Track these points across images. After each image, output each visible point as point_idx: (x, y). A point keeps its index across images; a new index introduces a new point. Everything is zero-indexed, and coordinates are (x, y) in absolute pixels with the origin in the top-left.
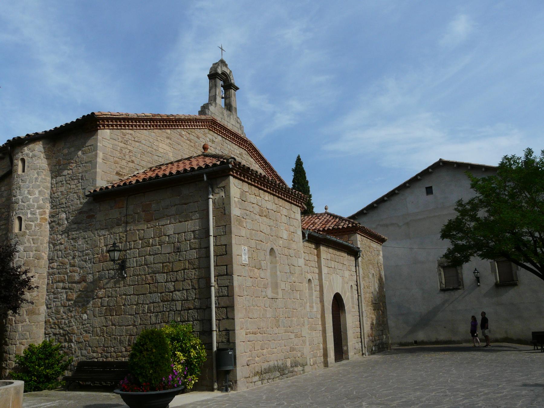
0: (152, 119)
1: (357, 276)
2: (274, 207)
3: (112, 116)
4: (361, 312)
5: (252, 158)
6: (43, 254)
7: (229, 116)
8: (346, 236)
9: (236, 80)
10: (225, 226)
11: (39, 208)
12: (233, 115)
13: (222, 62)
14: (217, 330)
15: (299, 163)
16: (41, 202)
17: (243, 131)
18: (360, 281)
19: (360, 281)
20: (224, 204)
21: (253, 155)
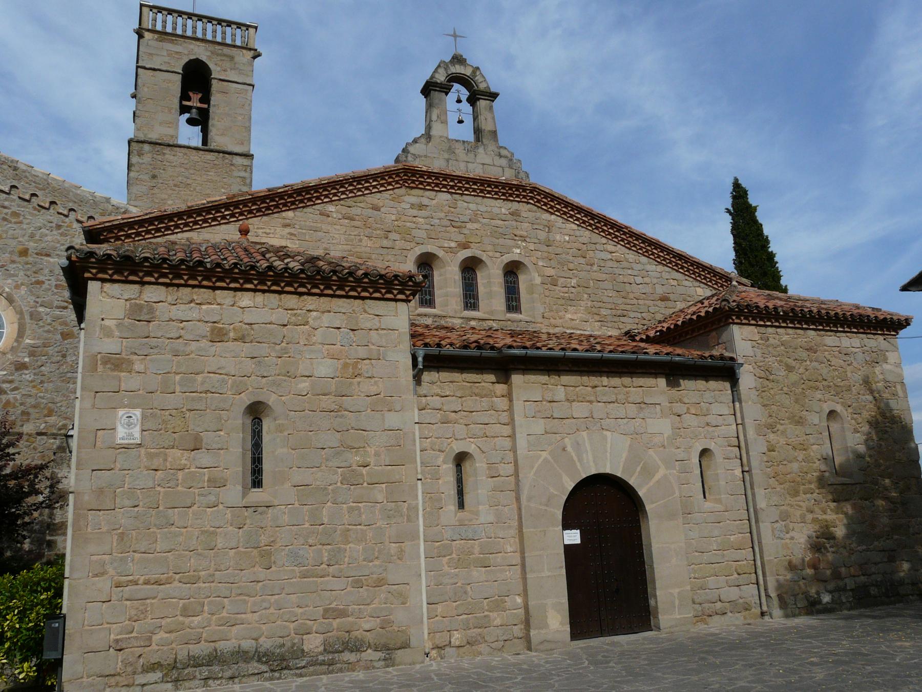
0: (226, 203)
1: (737, 425)
2: (279, 316)
3: (125, 221)
4: (752, 510)
5: (552, 214)
8: (714, 333)
9: (492, 78)
12: (484, 145)
13: (458, 59)
15: (739, 193)
18: (745, 436)
19: (745, 436)
21: (552, 207)
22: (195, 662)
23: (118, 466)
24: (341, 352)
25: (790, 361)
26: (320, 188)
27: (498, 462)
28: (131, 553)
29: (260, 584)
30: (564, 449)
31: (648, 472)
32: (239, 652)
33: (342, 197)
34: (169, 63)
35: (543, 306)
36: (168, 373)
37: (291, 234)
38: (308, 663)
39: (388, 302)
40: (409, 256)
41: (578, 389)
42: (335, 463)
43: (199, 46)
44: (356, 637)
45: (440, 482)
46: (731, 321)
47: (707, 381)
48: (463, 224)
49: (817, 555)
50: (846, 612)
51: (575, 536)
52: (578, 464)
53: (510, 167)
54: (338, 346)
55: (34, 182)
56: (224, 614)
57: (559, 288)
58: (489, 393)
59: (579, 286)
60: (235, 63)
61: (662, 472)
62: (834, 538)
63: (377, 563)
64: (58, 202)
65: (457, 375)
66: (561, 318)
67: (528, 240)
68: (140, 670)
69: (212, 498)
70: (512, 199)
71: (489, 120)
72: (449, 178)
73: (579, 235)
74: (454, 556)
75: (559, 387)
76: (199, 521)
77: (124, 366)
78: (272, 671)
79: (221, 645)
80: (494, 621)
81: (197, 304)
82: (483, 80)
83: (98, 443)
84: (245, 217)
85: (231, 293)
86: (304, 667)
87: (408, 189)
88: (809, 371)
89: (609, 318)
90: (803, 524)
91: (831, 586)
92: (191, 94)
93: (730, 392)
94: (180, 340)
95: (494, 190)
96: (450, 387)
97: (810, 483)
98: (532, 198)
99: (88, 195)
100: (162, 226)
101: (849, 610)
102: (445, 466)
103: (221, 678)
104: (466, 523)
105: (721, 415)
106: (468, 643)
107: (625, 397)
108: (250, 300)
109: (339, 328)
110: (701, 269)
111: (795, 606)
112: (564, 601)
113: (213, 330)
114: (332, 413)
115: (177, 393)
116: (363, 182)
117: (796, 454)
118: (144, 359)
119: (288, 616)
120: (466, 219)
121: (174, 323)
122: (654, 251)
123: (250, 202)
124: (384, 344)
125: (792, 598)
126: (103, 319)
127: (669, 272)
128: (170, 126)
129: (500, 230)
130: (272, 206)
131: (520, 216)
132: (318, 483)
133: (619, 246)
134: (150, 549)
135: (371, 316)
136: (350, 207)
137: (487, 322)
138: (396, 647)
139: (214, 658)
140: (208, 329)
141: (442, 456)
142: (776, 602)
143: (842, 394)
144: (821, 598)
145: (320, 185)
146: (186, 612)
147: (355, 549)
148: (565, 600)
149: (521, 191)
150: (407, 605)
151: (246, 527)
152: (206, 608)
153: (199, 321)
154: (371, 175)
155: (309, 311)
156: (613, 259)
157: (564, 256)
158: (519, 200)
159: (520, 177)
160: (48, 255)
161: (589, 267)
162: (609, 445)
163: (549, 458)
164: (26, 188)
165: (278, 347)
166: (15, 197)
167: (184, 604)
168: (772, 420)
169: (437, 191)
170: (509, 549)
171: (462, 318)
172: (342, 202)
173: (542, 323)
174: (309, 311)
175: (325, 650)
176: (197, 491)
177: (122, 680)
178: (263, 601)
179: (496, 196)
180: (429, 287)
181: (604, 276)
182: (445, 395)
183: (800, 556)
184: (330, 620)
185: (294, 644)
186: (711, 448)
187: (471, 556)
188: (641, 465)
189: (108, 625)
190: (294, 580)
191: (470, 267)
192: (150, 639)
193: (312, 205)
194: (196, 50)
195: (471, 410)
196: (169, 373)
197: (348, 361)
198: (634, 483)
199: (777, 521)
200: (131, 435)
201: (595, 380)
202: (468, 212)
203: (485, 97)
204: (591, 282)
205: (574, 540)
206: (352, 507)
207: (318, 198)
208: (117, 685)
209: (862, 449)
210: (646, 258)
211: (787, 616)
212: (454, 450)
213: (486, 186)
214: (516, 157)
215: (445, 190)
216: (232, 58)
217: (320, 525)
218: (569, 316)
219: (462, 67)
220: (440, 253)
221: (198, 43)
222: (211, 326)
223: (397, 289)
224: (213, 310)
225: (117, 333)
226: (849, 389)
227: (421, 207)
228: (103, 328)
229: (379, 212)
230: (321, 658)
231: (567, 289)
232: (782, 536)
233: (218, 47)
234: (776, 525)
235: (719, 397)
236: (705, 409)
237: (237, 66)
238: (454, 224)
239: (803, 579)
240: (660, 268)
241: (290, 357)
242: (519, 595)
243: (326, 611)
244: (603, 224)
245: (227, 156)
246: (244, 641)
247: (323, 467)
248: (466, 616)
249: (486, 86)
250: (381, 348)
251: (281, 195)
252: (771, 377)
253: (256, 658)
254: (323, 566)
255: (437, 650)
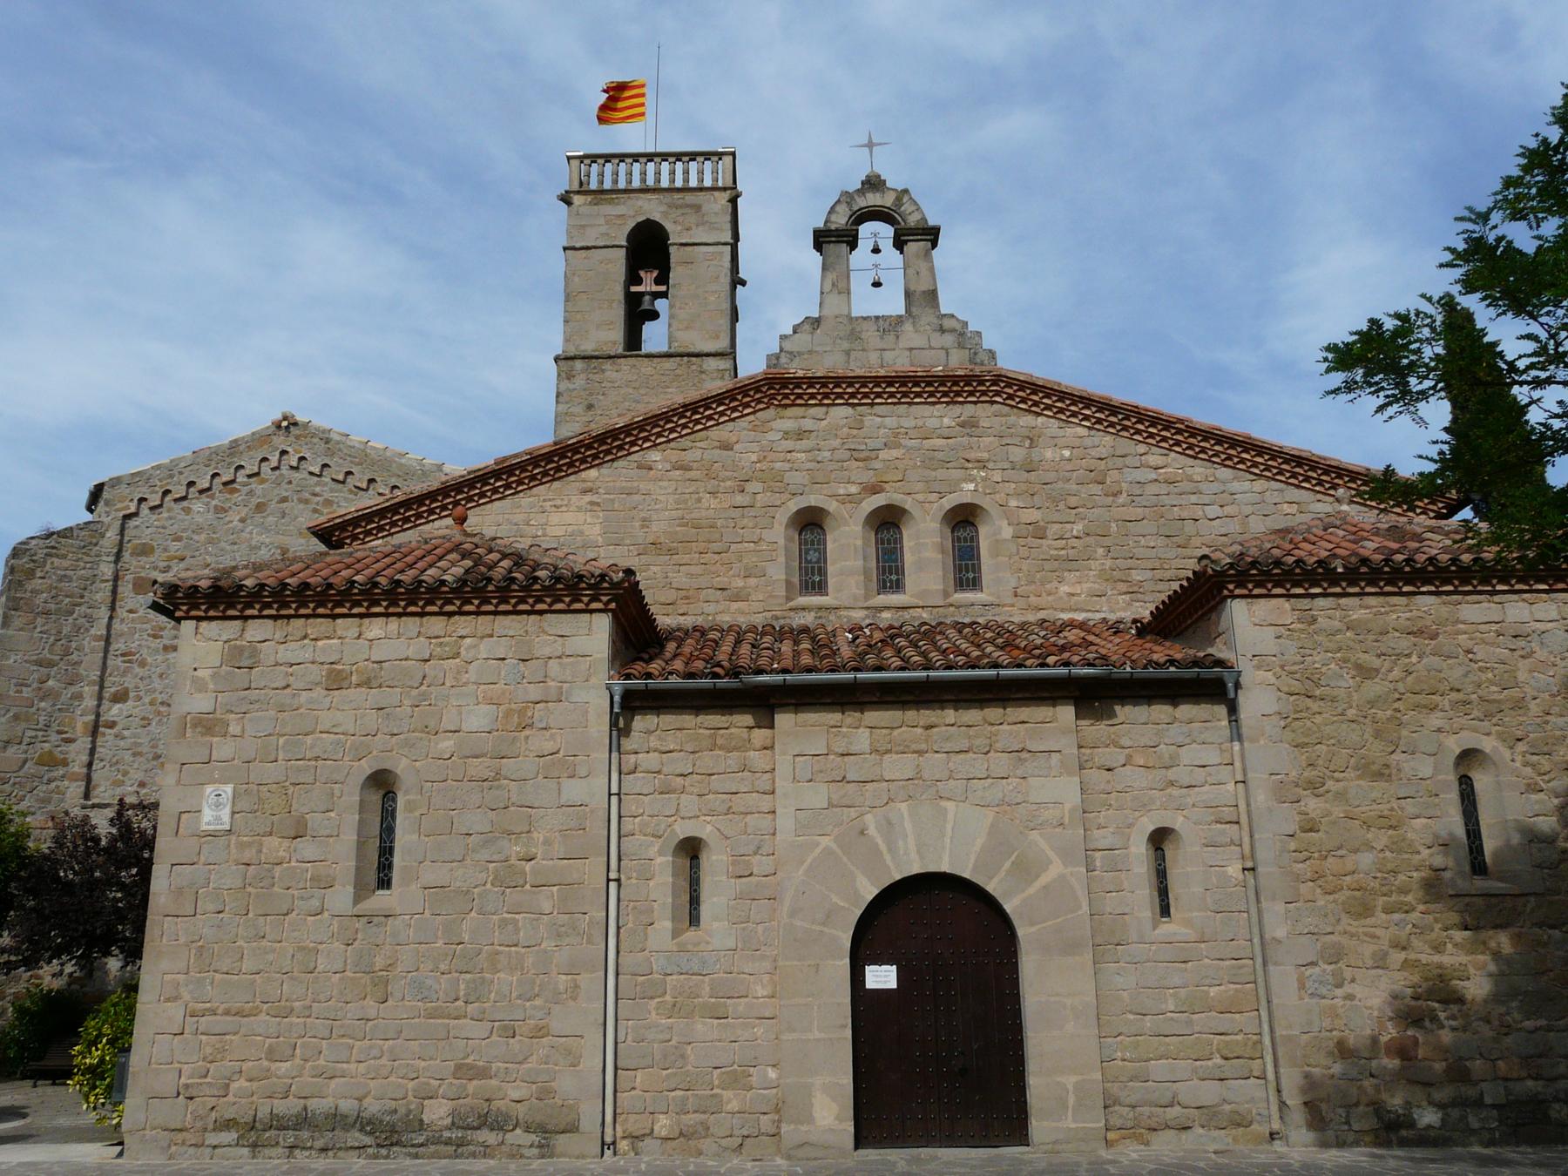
0: (495, 471)
2: (420, 647)
3: (360, 513)
12: (914, 317)
13: (874, 183)
21: (1036, 404)
22: (279, 1123)
23: (203, 858)
24: (503, 693)
25: (1370, 660)
26: (634, 429)
27: (751, 853)
28: (211, 973)
29: (370, 1023)
30: (862, 833)
31: (1026, 870)
32: (335, 1114)
33: (671, 437)
34: (607, 234)
35: (1016, 575)
36: (270, 735)
37: (592, 503)
38: (428, 1140)
39: (578, 615)
40: (777, 516)
41: (896, 732)
42: (484, 855)
43: (650, 200)
44: (498, 1109)
45: (651, 883)
46: (1226, 592)
47: (1175, 705)
48: (873, 454)
49: (1409, 1033)
50: (1477, 1149)
51: (886, 976)
52: (887, 857)
53: (961, 346)
54: (500, 686)
55: (350, 456)
56: (322, 1062)
57: (1050, 542)
58: (740, 744)
59: (1088, 534)
60: (704, 215)
61: (1055, 869)
62: (1460, 1000)
63: (538, 1002)
64: (377, 479)
65: (687, 717)
66: (1049, 594)
67: (990, 465)
68: (211, 1126)
69: (315, 903)
70: (961, 399)
71: (924, 273)
72: (844, 382)
73: (1090, 444)
74: (668, 998)
75: (861, 730)
76: (296, 934)
77: (217, 729)
78: (379, 1146)
79: (313, 1104)
80: (727, 1104)
81: (312, 640)
82: (914, 208)
83: (181, 830)
84: (525, 487)
85: (357, 620)
86: (422, 1145)
87: (779, 409)
88: (1414, 674)
89: (1148, 586)
90: (1380, 972)
91: (1440, 1095)
92: (642, 273)
93: (1225, 723)
94: (288, 691)
95: (927, 389)
96: (676, 737)
97: (1403, 891)
98: (997, 394)
99: (415, 464)
100: (411, 513)
101: (1487, 1147)
102: (659, 860)
103: (311, 1148)
104: (690, 947)
105: (1204, 766)
106: (681, 1134)
107: (988, 741)
108: (381, 629)
109: (504, 659)
110: (1347, 479)
111: (1346, 1127)
112: (845, 1081)
113: (330, 672)
114: (485, 783)
115: (280, 762)
116: (701, 410)
117: (1370, 836)
118: (242, 718)
119: (405, 1071)
120: (872, 444)
121: (282, 667)
122: (1244, 455)
123: (529, 465)
124: (569, 678)
125: (1341, 1111)
126: (195, 669)
127: (1281, 491)
128: (611, 327)
129: (939, 455)
130: (564, 465)
131: (978, 427)
132: (458, 884)
133: (1173, 455)
134: (233, 969)
135: (552, 638)
136: (685, 450)
137: (911, 611)
138: (557, 1129)
139: (303, 1121)
140: (324, 673)
141: (658, 844)
142: (1298, 1116)
143: (1499, 716)
144: (1415, 1116)
145: (632, 424)
146: (271, 1055)
147: (505, 979)
148: (847, 1080)
149: (975, 384)
150: (577, 1068)
151: (356, 943)
152: (298, 1051)
153: (313, 663)
154: (712, 397)
155: (462, 637)
156: (1160, 478)
157: (1060, 485)
158: (974, 399)
159: (978, 361)
161: (1111, 498)
162: (949, 827)
163: (834, 846)
164: (340, 465)
165: (415, 692)
166: (328, 480)
167: (270, 1046)
168: (1313, 773)
169: (828, 405)
170: (761, 992)
171: (868, 608)
172: (672, 445)
173: (1013, 606)
174: (462, 637)
175: (453, 1123)
176: (296, 892)
177: (191, 1137)
178: (371, 1047)
179: (933, 399)
180: (818, 561)
181: (1138, 512)
182: (668, 749)
183: (1369, 1032)
184: (464, 1081)
185: (410, 1111)
186: (1176, 828)
187: (696, 1000)
188: (1013, 858)
189: (179, 1065)
190: (417, 1020)
191: (887, 522)
192: (228, 1086)
193: (626, 455)
194: (646, 206)
195: (710, 772)
196: (270, 735)
197: (513, 706)
198: (994, 889)
199: (1313, 964)
200: (218, 819)
201: (927, 715)
202: (882, 431)
203: (919, 237)
204: (1113, 525)
205: (885, 982)
206: (504, 920)
207: (633, 444)
208: (183, 1143)
209: (1547, 824)
210: (1230, 470)
211: (1324, 1145)
212: (676, 834)
213: (910, 385)
214: (971, 328)
215: (841, 401)
216: (697, 208)
217: (458, 944)
218: (1064, 589)
219: (878, 195)
220: (832, 506)
221: (649, 196)
222: (328, 669)
223: (586, 595)
224: (330, 646)
225: (211, 686)
226: (1519, 705)
227: (801, 434)
228: (195, 680)
229: (730, 453)
230: (446, 1134)
231: (1064, 541)
232: (1323, 991)
233: (677, 196)
234: (1310, 971)
235: (1201, 733)
236: (1167, 756)
237: (705, 219)
238: (856, 454)
239: (1372, 1075)
240: (1260, 485)
241: (430, 705)
242: (774, 1066)
243: (458, 1067)
244: (1134, 420)
245: (694, 359)
246: (343, 1100)
247: (468, 861)
248: (682, 1092)
249: (919, 217)
250: (565, 685)
251: (575, 449)
252: (1317, 693)
253: (358, 1125)
254: (457, 1003)
255: (630, 1140)
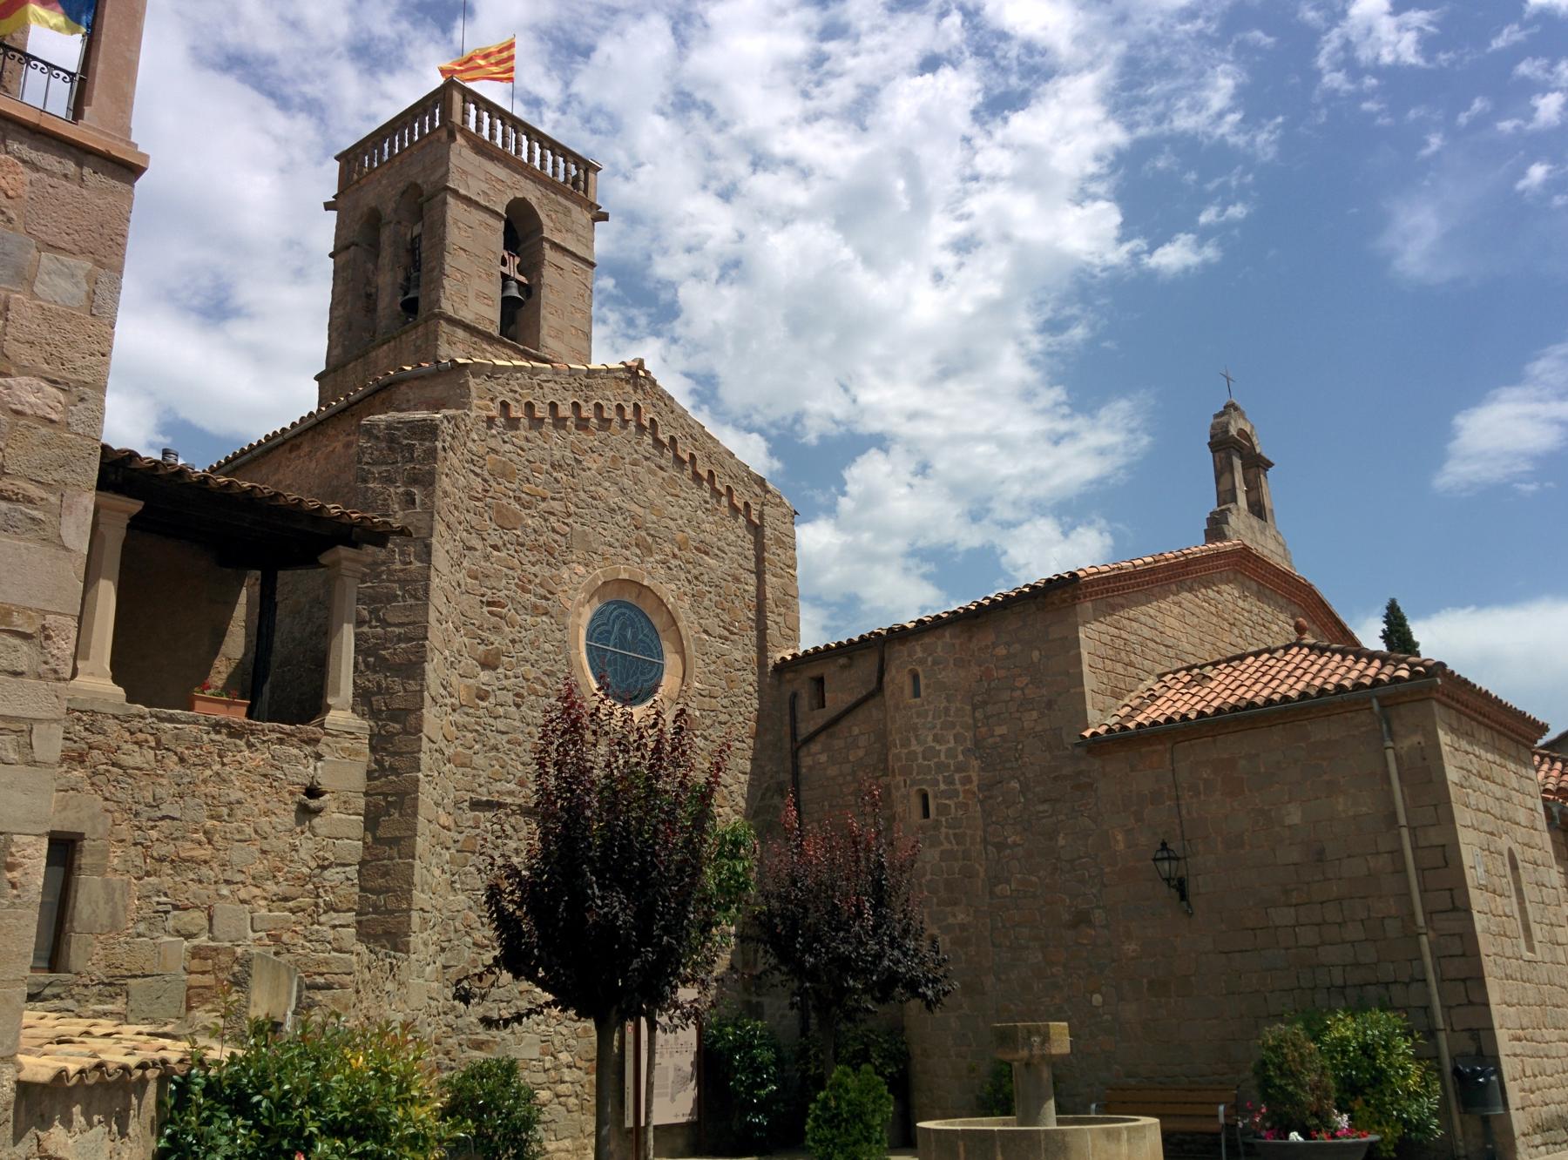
6: (977, 866)
7: (1263, 532)
10: (1435, 806)
11: (959, 769)
13: (1231, 407)
14: (1448, 1029)
16: (961, 758)
17: (1290, 562)
20: (1424, 759)
160: (707, 554)
216: (567, 212)
